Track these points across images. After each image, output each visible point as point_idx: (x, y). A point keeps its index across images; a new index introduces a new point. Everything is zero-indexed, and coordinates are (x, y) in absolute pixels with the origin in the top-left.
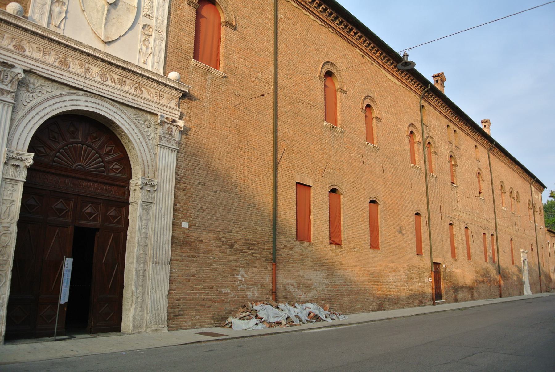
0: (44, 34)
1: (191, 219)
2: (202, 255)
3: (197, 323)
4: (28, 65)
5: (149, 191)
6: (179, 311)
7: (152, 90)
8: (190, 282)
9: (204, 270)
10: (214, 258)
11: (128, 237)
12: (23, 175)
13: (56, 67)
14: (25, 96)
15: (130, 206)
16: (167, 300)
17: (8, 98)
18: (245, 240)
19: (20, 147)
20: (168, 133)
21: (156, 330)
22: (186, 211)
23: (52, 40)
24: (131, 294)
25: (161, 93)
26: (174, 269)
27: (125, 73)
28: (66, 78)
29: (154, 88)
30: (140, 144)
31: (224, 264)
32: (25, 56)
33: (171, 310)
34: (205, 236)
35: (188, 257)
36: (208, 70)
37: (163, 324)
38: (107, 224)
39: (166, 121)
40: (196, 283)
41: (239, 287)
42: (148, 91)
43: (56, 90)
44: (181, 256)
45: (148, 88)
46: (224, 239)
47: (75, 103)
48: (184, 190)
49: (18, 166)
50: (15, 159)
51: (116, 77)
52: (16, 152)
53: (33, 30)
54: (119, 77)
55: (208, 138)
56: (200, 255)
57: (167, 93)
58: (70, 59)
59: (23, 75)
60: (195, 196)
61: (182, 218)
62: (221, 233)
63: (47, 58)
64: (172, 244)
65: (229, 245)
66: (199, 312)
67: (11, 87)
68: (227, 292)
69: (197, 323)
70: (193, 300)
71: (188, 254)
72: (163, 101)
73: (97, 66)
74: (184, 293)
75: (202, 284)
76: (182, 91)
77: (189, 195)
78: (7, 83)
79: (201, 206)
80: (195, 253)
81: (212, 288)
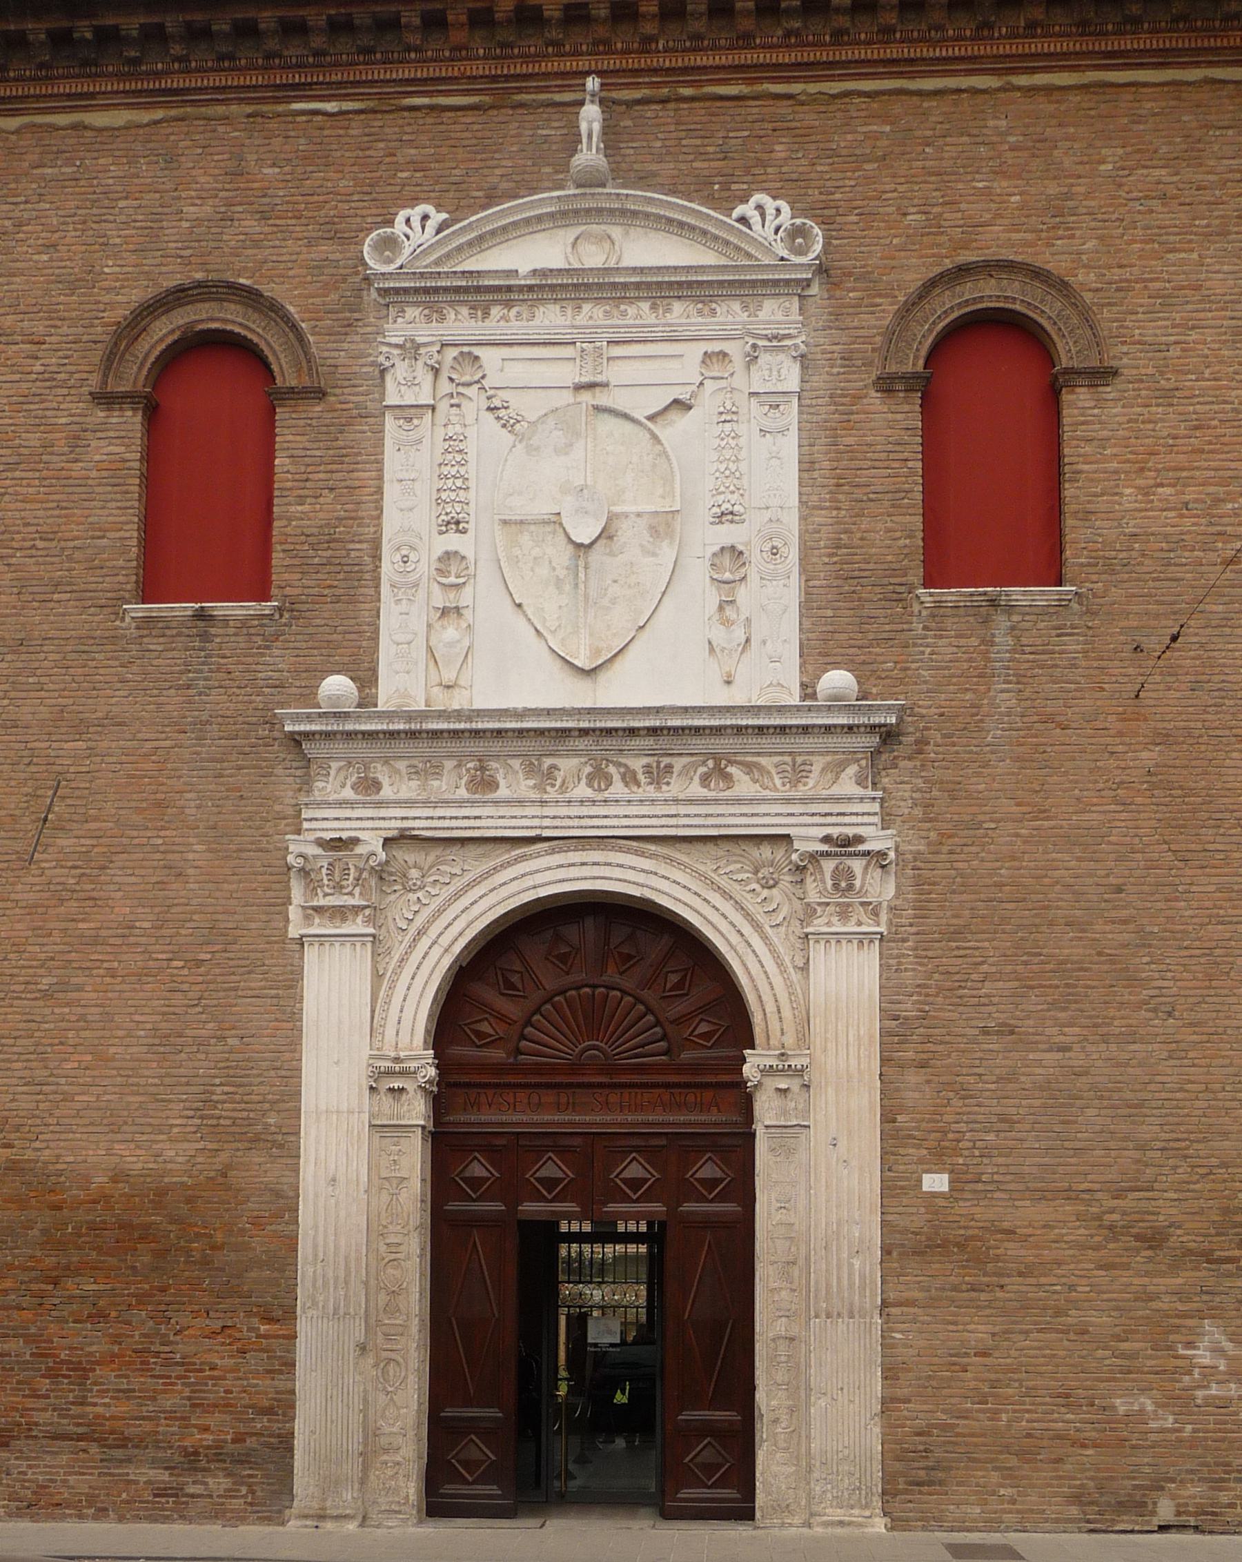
0: (413, 726)
1: (961, 1161)
2: (1015, 1284)
3: (1004, 1511)
4: (393, 824)
5: (786, 1091)
7: (763, 761)
9: (1027, 1332)
10: (1072, 1288)
12: (417, 1111)
13: (461, 803)
14: (400, 907)
16: (877, 1430)
17: (358, 926)
18: (1226, 1211)
19: (404, 1039)
20: (836, 886)
23: (436, 734)
25: (799, 760)
27: (664, 742)
28: (492, 821)
29: (770, 754)
30: (742, 948)
31: (1117, 1309)
32: (380, 804)
33: (898, 1466)
34: (1028, 1213)
35: (955, 1289)
36: (993, 603)
37: (867, 1506)
38: (688, 1207)
39: (825, 848)
40: (993, 1376)
41: (1200, 1393)
42: (749, 768)
43: (473, 864)
45: (749, 759)
46: (1116, 1217)
47: (528, 881)
49: (402, 1090)
50: (390, 1073)
51: (637, 764)
52: (393, 1054)
53: (385, 727)
55: (1014, 859)
56: (1006, 1280)
57: (821, 754)
58: (494, 765)
59: (382, 856)
60: (972, 1079)
61: (921, 1161)
62: (1099, 1195)
63: (436, 783)
65: (1138, 1238)
66: (1011, 1477)
67: (361, 894)
68: (1142, 1411)
69: (1004, 1511)
72: (811, 783)
73: (576, 753)
74: (944, 1411)
76: (873, 727)
77: (943, 1079)
78: (350, 888)
79: (998, 1110)
81: (1068, 1396)
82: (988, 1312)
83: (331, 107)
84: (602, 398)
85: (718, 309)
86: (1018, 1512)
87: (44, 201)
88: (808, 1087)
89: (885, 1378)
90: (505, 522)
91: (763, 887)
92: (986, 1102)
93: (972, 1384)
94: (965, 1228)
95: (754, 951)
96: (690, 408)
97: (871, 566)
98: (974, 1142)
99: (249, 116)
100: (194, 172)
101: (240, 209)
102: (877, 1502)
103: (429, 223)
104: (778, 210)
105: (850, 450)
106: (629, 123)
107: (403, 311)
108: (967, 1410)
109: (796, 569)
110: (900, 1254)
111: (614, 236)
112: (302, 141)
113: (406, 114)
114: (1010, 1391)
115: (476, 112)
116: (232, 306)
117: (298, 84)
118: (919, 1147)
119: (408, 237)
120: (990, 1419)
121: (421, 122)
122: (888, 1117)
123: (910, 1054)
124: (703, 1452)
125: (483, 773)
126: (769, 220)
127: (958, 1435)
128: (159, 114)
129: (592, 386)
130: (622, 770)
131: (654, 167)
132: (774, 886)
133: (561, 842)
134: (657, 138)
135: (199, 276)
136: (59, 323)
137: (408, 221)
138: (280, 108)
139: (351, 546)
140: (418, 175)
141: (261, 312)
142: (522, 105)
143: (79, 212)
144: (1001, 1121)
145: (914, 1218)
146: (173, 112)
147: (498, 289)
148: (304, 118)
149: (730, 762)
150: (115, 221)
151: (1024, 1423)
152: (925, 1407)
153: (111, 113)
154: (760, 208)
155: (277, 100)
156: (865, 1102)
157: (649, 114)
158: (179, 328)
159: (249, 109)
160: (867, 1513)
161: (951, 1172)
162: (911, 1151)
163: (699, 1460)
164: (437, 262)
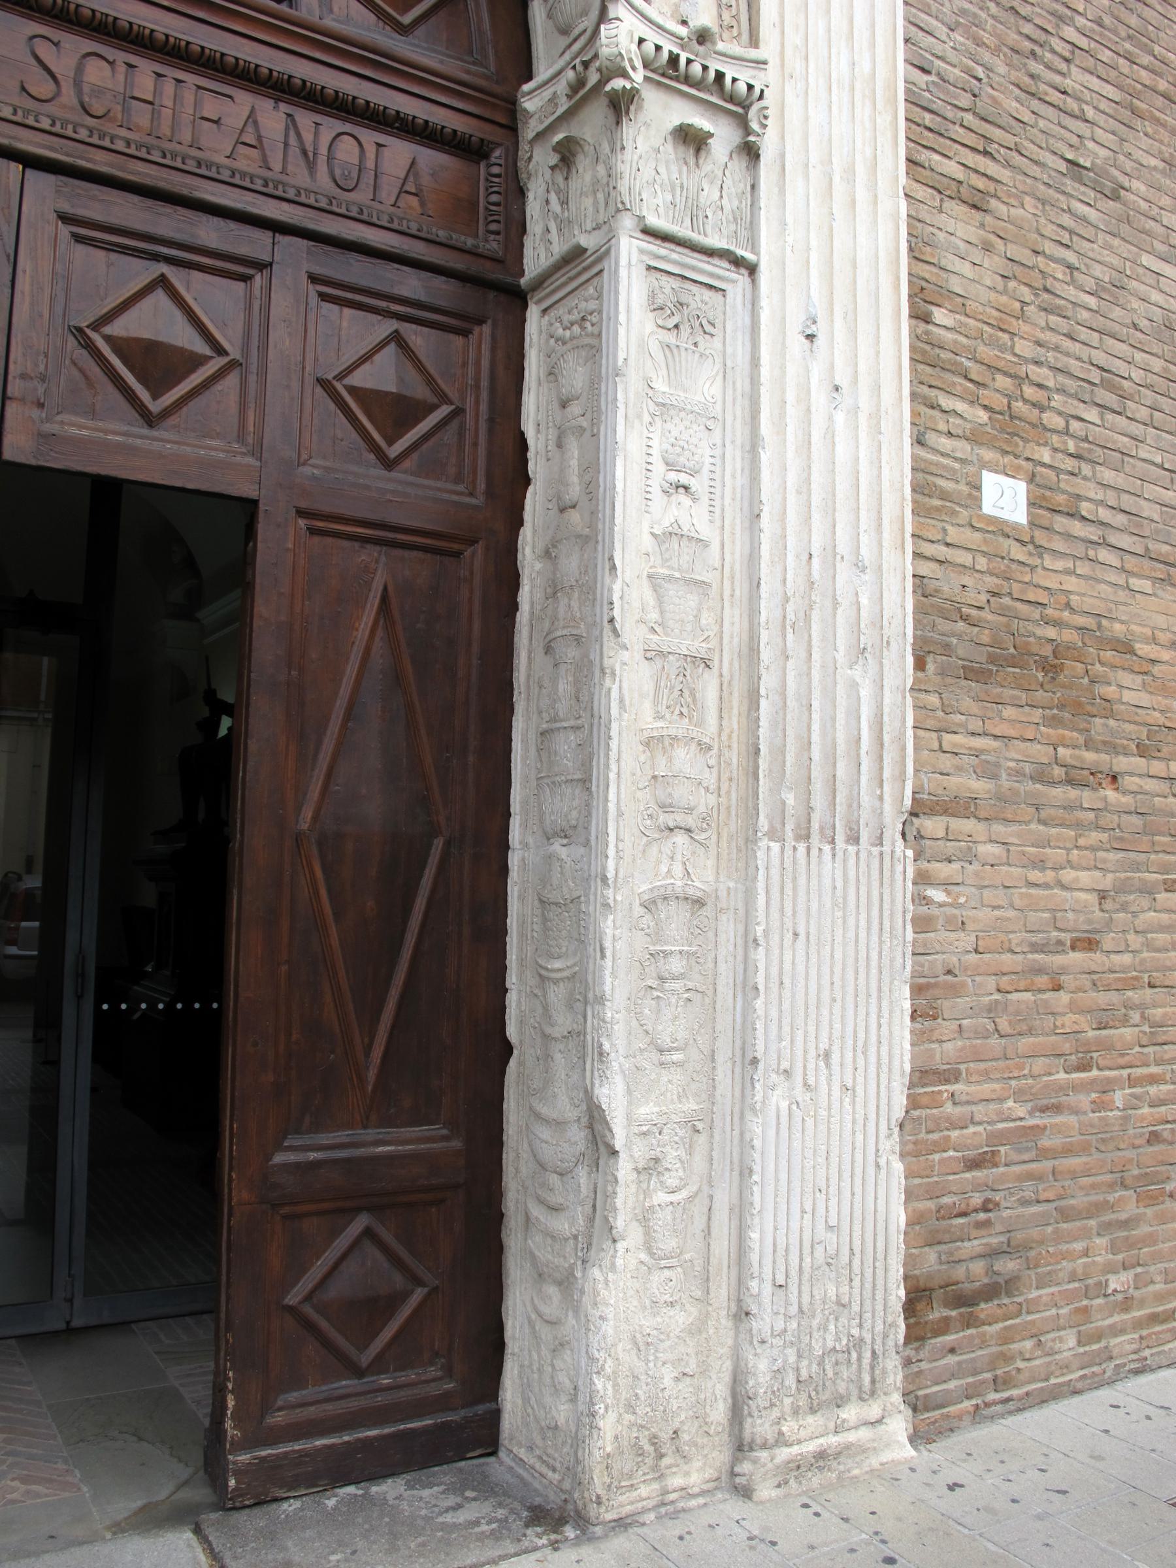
1: (1046, 456)
6: (992, 1254)
8: (1064, 997)
9: (1148, 890)
11: (526, 596)
15: (533, 313)
22: (1002, 381)
24: (578, 1136)
26: (947, 885)
35: (1041, 777)
40: (1103, 998)
44: (989, 771)
56: (1122, 763)
64: (920, 665)
70: (1085, 1148)
71: (1041, 752)
74: (1019, 1095)
75: (1142, 1007)
77: (1013, 251)
80: (1088, 745)
82: (1094, 837)
86: (1138, 1324)
88: (750, 152)
89: (914, 1016)
92: (1084, 334)
93: (1069, 1021)
94: (1057, 623)
102: (894, 1374)
108: (1063, 1089)
110: (942, 672)
114: (1127, 1033)
118: (974, 401)
123: (951, 168)
124: (339, 1262)
127: (1044, 1154)
144: (1107, 385)
145: (967, 580)
151: (1146, 1110)
161: (1031, 479)
162: (960, 406)
163: (337, 1290)
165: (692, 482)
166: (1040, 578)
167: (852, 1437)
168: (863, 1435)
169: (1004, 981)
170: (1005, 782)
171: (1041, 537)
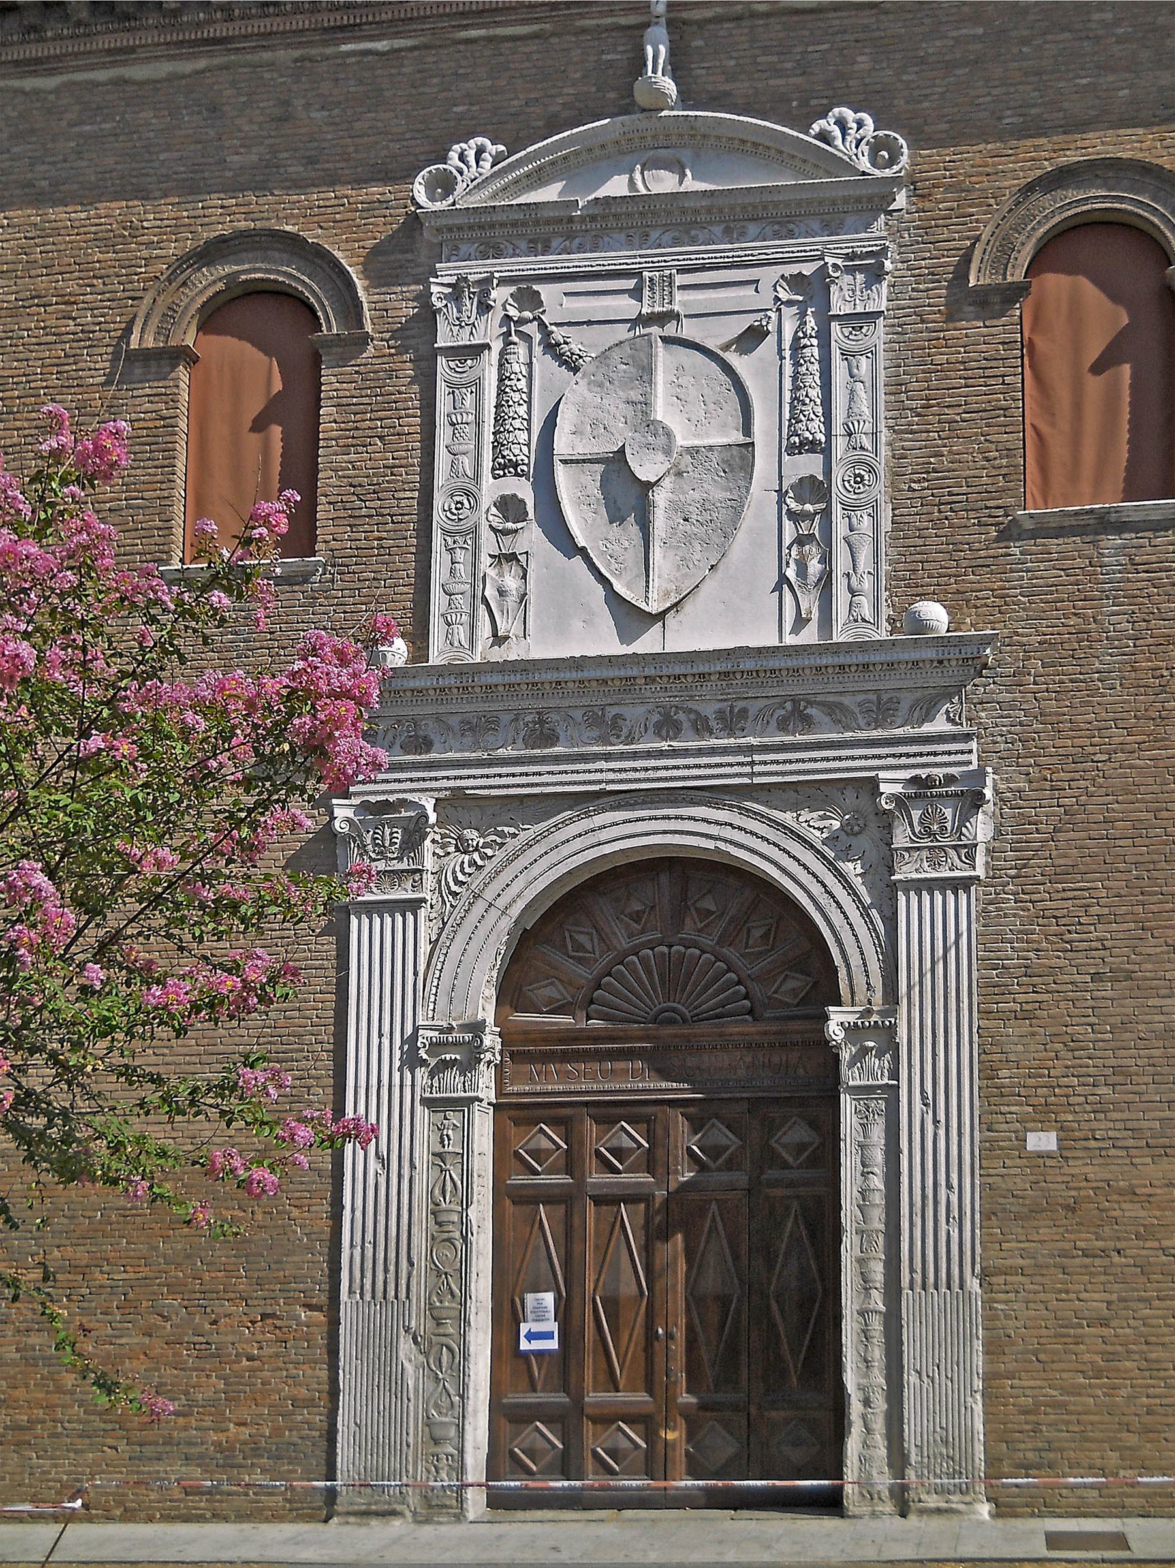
1: (1070, 1117)
16: (979, 1408)
21: (939, 1511)
25: (885, 697)
30: (824, 900)
48: (1027, 1016)
51: (709, 710)
54: (719, 705)
58: (554, 717)
83: (381, 45)
84: (670, 329)
85: (796, 230)
87: (82, 159)
89: (986, 1353)
90: (565, 462)
91: (848, 834)
95: (837, 903)
96: (768, 332)
97: (964, 489)
98: (1085, 1096)
99: (296, 60)
100: (238, 122)
101: (286, 155)
103: (486, 155)
104: (860, 124)
105: (940, 369)
106: (700, 43)
107: (457, 248)
109: (882, 499)
111: (684, 160)
112: (352, 83)
113: (462, 47)
115: (537, 41)
116: (277, 255)
117: (346, 26)
119: (461, 173)
120: (1105, 1394)
121: (478, 54)
122: (988, 1072)
125: (542, 726)
126: (851, 134)
128: (202, 63)
129: (661, 319)
130: (692, 716)
131: (727, 87)
132: (859, 833)
133: (628, 795)
134: (731, 58)
135: (243, 225)
136: (95, 281)
137: (462, 157)
138: (329, 51)
139: (401, 495)
140: (474, 108)
141: (306, 259)
142: (584, 31)
143: (119, 167)
145: (1018, 1180)
146: (216, 61)
147: (559, 221)
148: (353, 60)
149: (810, 703)
150: (155, 174)
152: (1032, 1383)
153: (152, 66)
154: (841, 123)
155: (326, 43)
156: (962, 1057)
157: (721, 33)
158: (220, 280)
159: (297, 53)
160: (968, 1499)
162: (1013, 1109)
164: (494, 196)
165: (876, 1170)
166: (1066, 1170)
167: (954, 1506)
168: (961, 1507)
169: (1042, 1340)
170: (1041, 1260)
171: (1065, 1153)
